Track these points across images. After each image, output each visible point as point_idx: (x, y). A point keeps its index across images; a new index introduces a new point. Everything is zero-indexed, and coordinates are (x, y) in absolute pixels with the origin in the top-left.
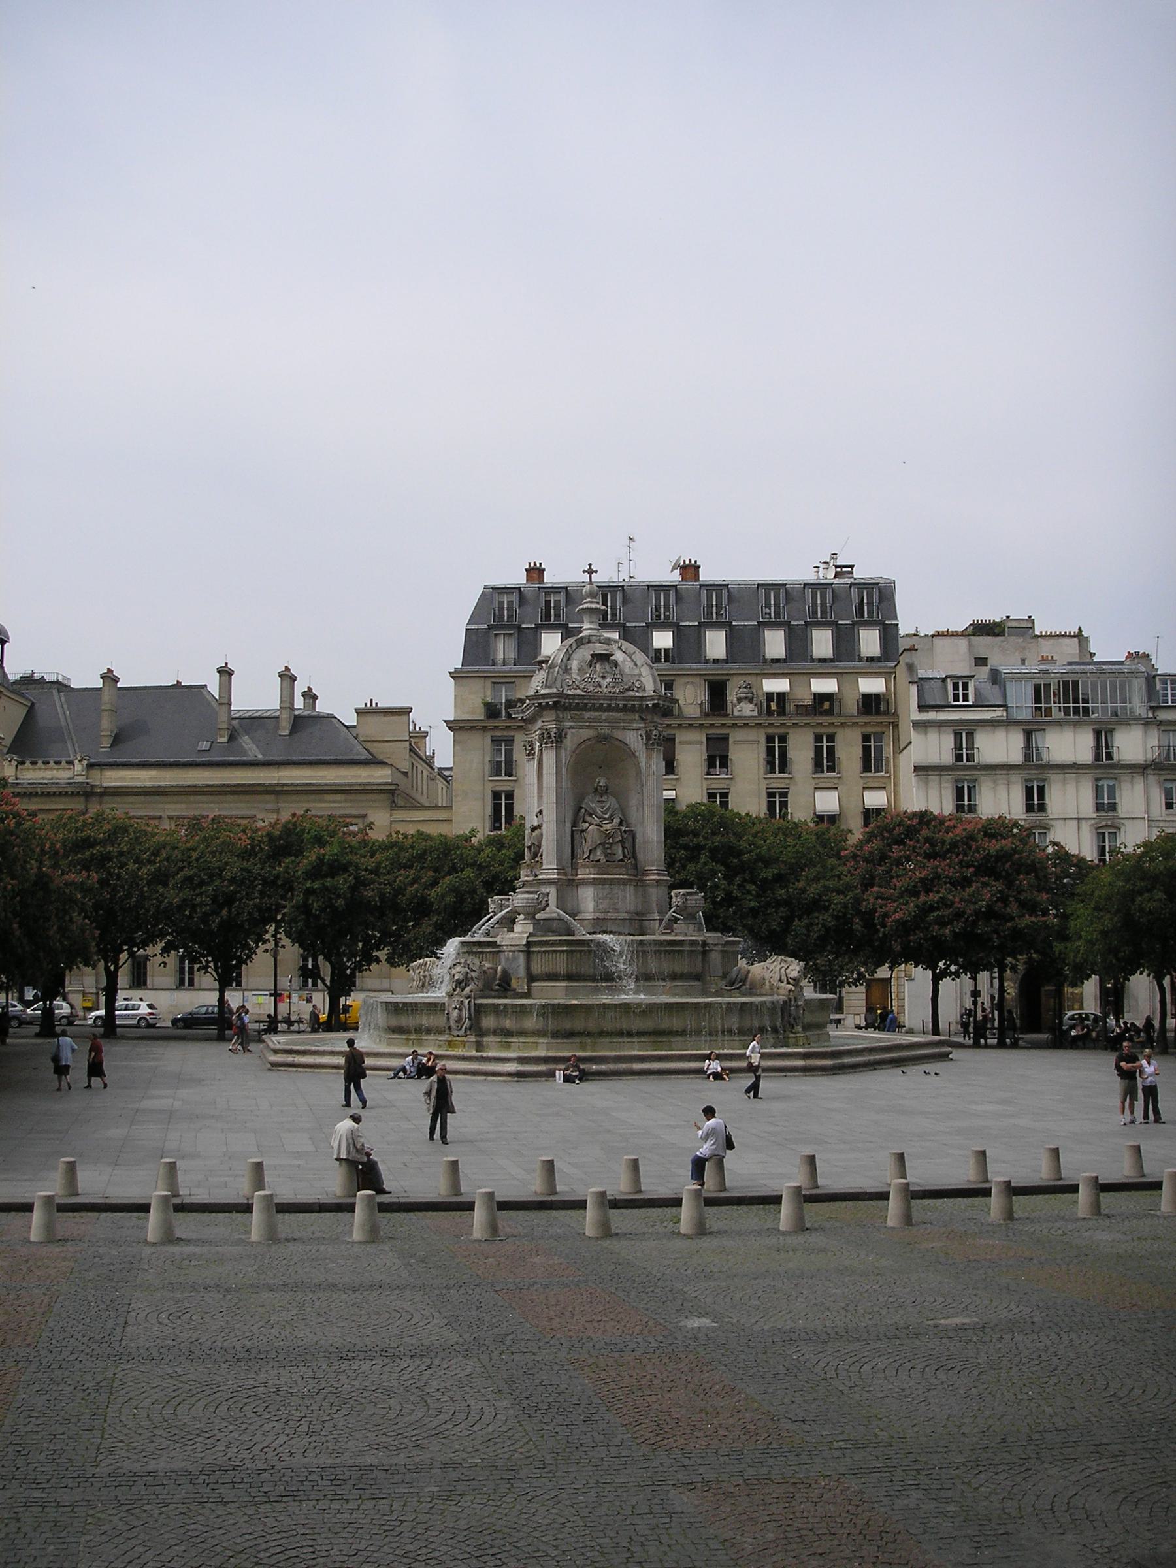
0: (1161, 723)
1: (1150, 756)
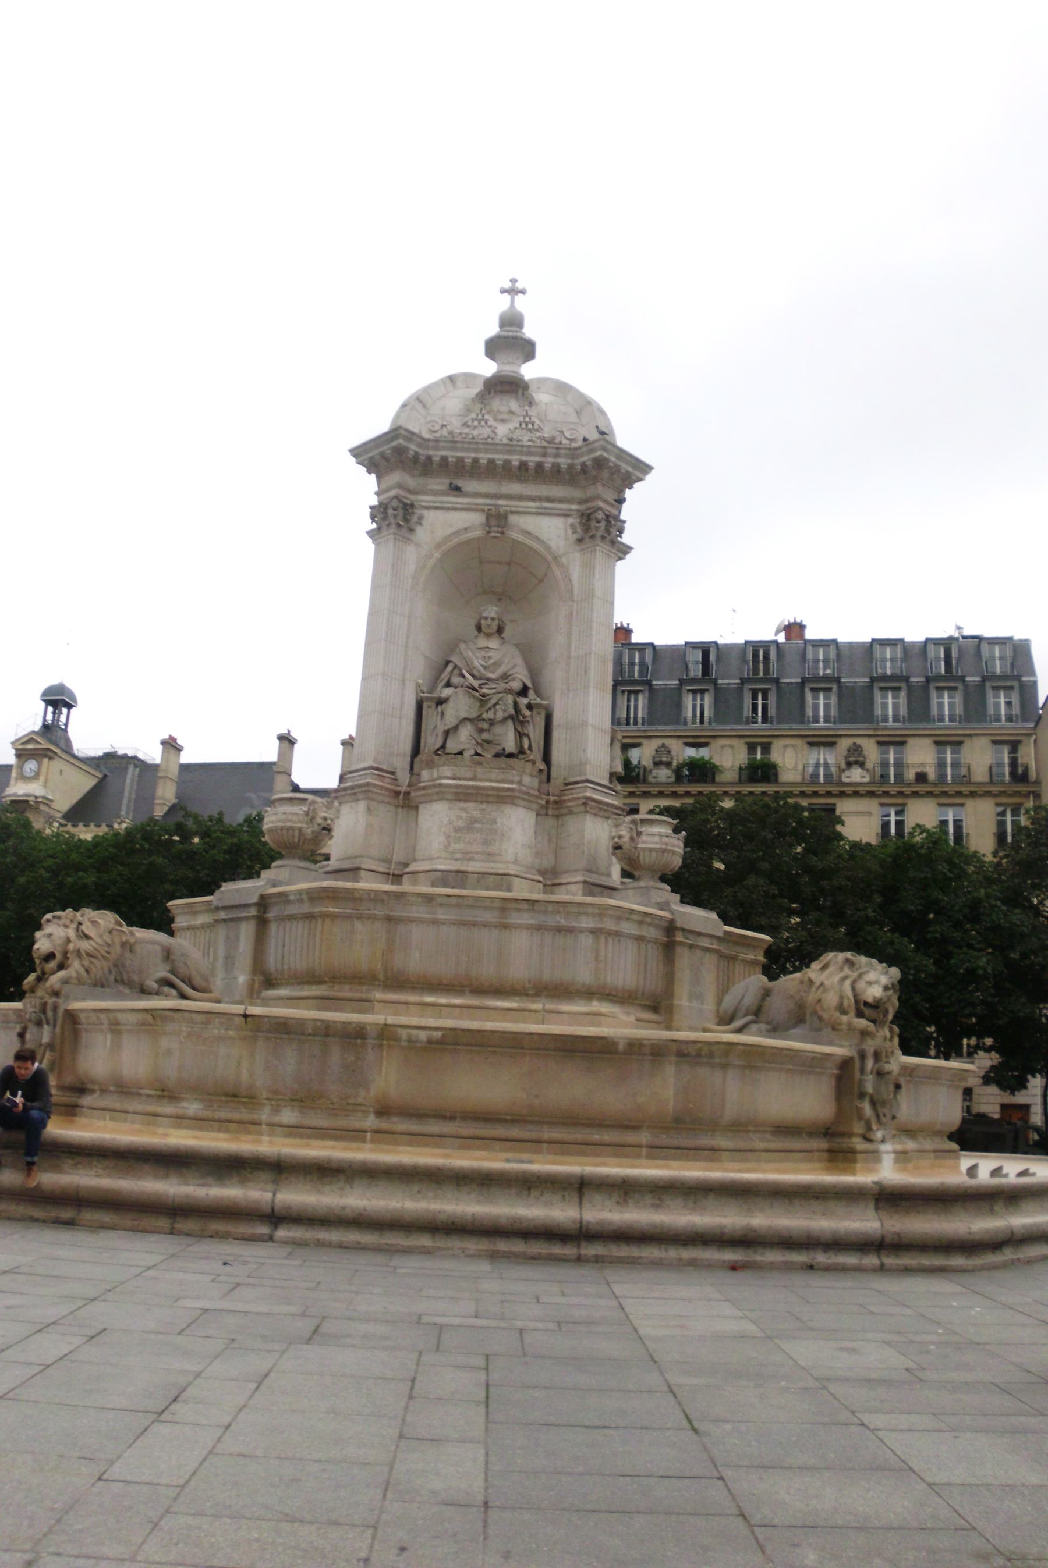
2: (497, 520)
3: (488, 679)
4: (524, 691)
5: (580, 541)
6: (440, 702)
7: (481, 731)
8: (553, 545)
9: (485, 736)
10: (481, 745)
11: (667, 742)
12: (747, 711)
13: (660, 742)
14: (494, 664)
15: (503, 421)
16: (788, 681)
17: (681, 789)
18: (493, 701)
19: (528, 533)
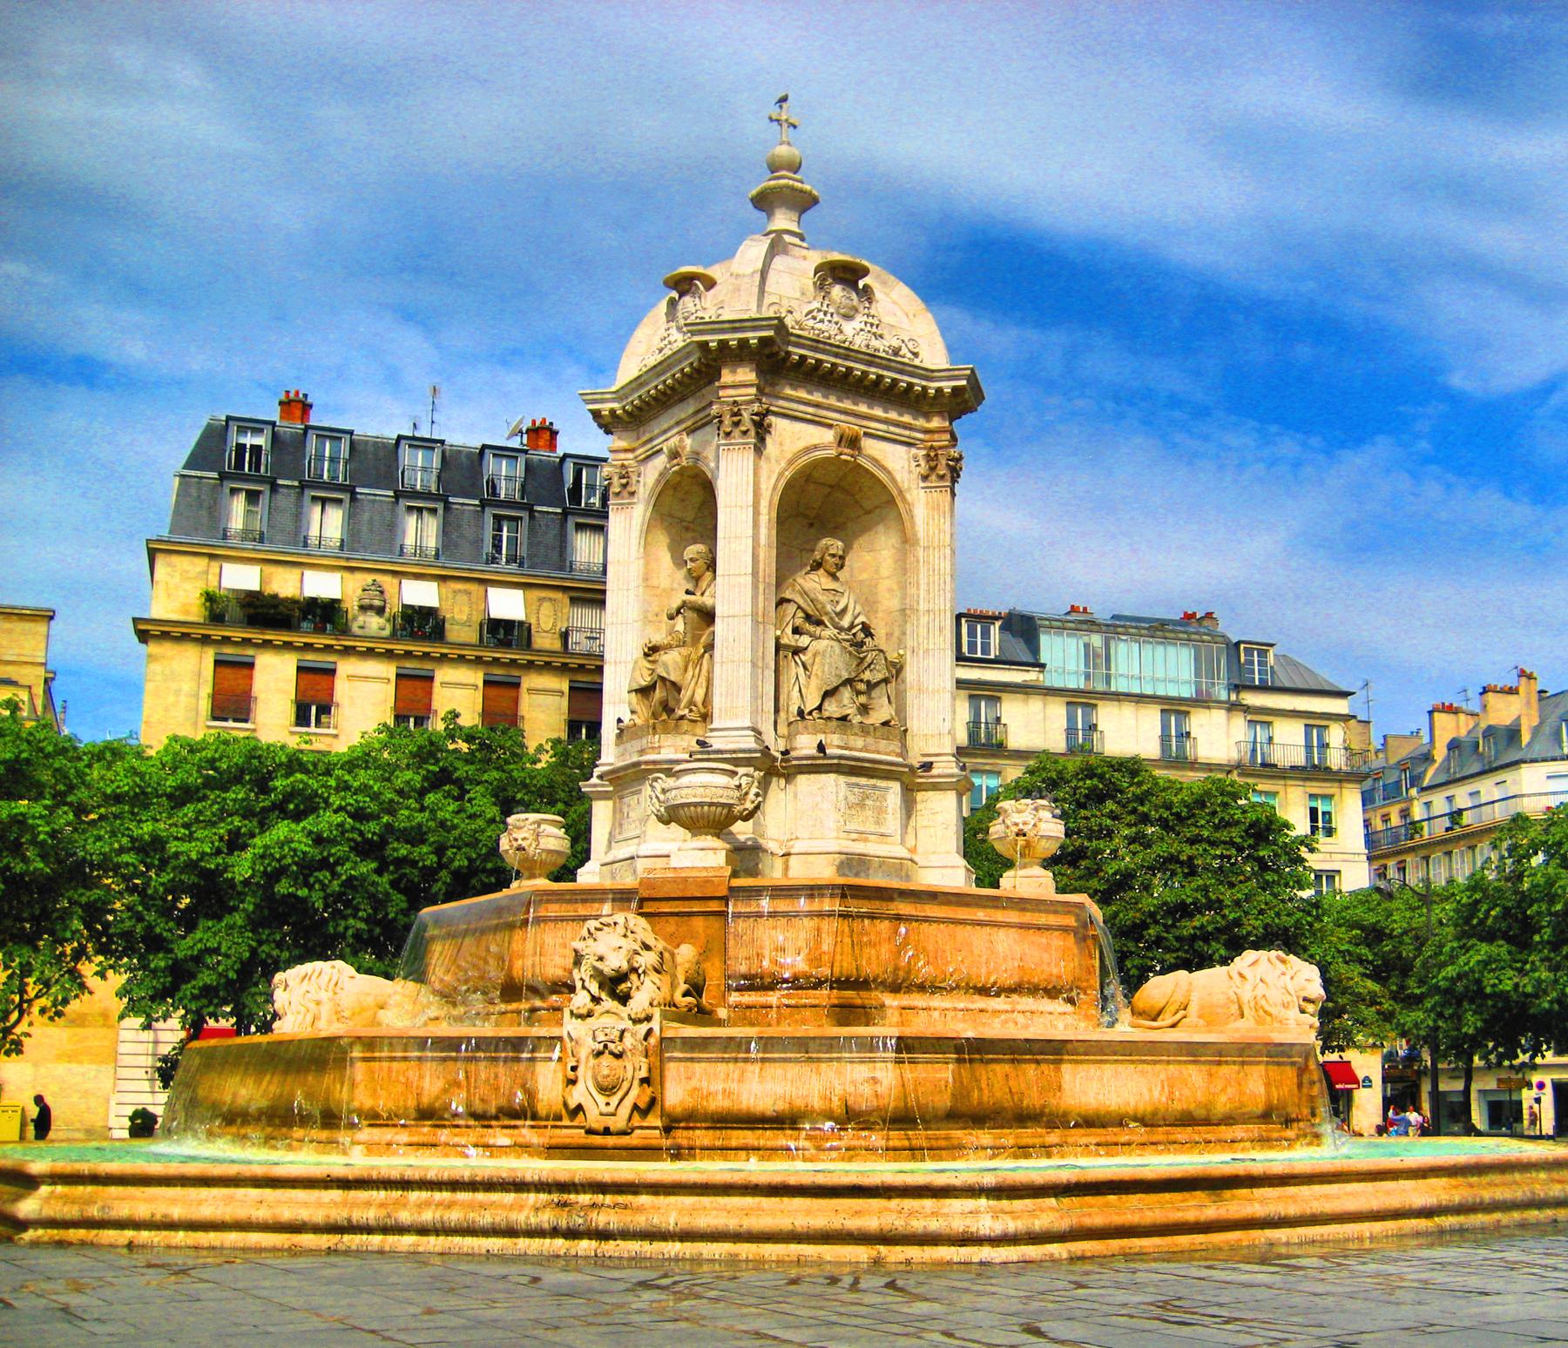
0: (1247, 709)
1: (1234, 756)
2: (853, 442)
5: (925, 478)
7: (859, 693)
8: (898, 478)
11: (380, 578)
12: (488, 547)
13: (369, 578)
15: (848, 317)
16: (545, 509)
17: (399, 648)
18: (868, 660)
19: (875, 462)
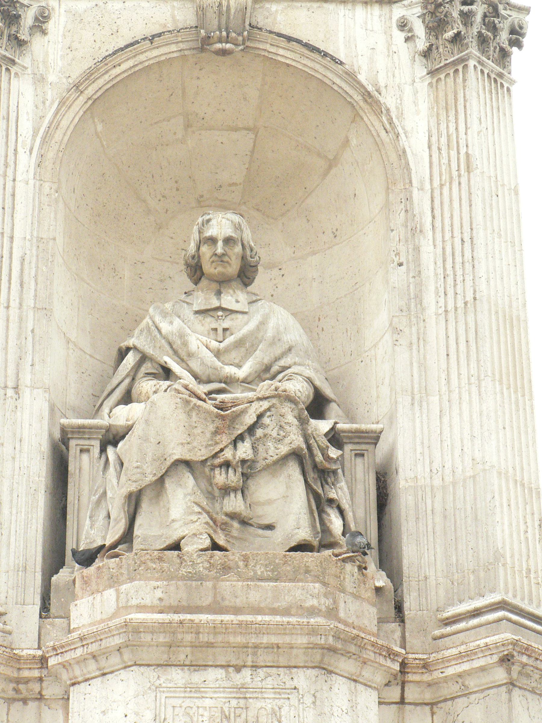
3: (229, 381)
4: (318, 406)
6: (112, 438)
9: (235, 503)
10: (224, 527)
14: (239, 344)
18: (249, 419)
